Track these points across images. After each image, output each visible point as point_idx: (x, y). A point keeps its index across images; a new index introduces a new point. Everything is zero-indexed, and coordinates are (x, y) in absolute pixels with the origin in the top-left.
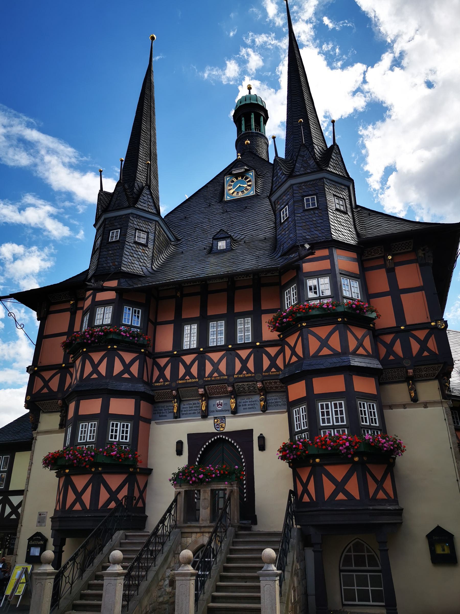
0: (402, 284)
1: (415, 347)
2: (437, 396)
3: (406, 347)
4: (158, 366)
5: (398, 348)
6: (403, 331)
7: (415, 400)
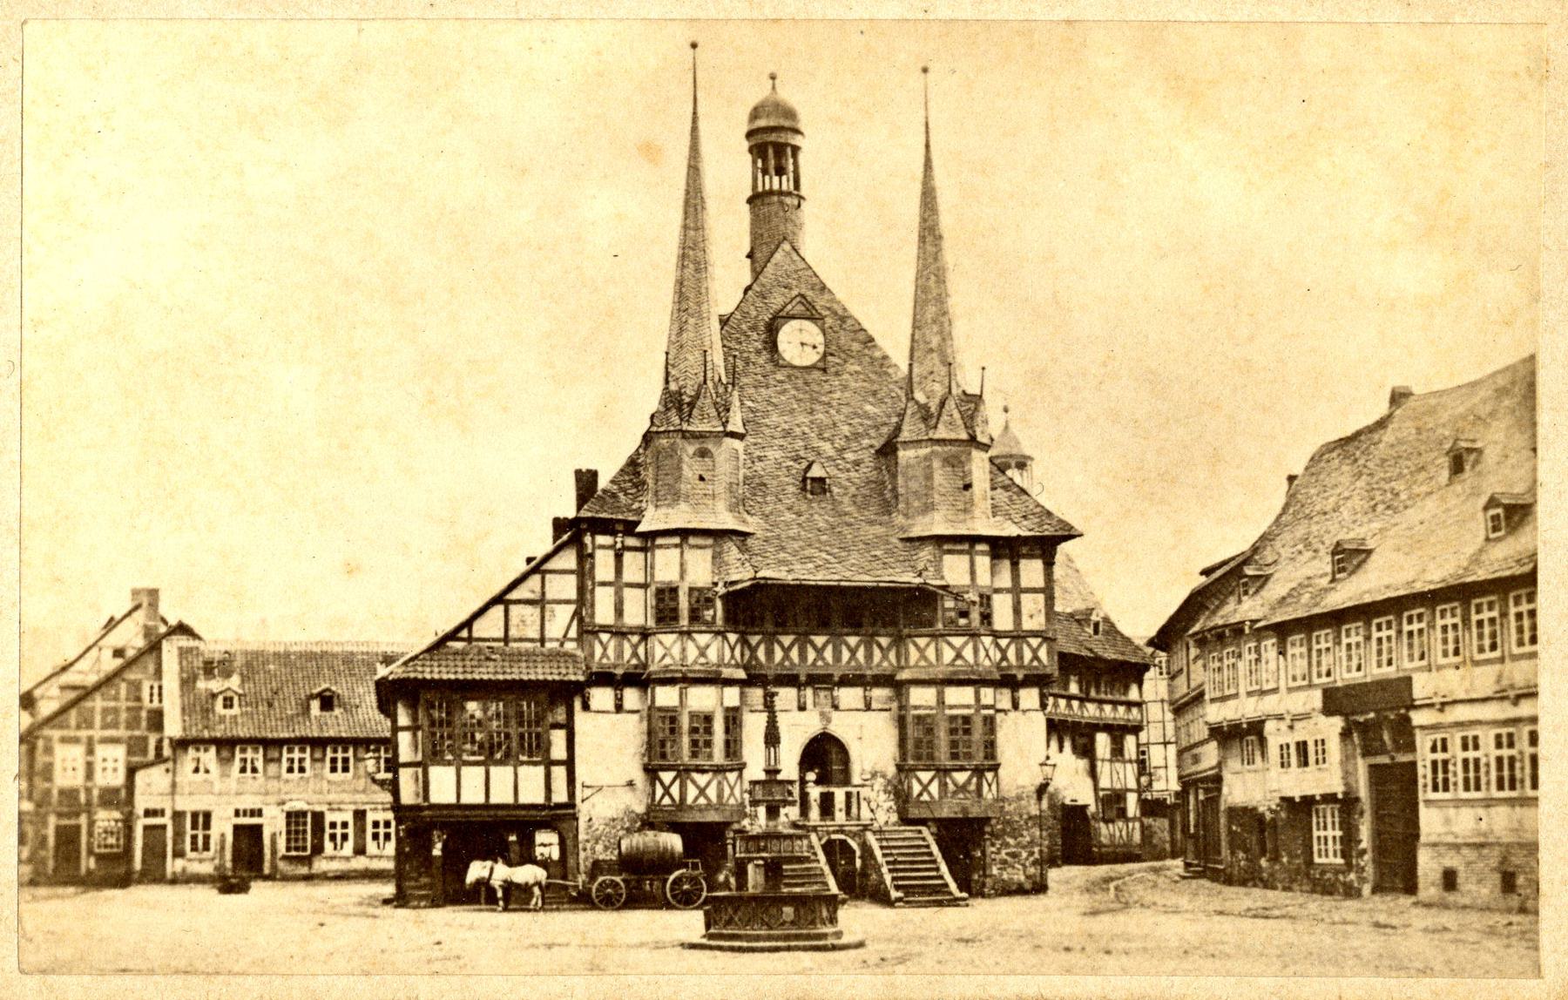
0: (1024, 583)
1: (1028, 655)
2: (1036, 704)
3: (1020, 656)
4: (749, 646)
5: (1011, 654)
6: (1018, 636)
7: (1015, 706)
